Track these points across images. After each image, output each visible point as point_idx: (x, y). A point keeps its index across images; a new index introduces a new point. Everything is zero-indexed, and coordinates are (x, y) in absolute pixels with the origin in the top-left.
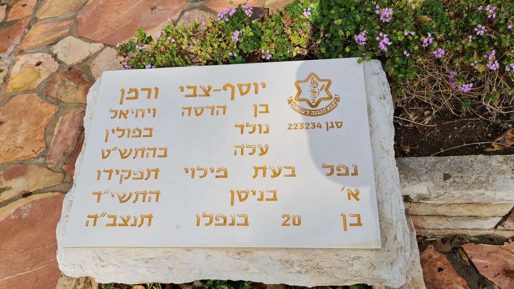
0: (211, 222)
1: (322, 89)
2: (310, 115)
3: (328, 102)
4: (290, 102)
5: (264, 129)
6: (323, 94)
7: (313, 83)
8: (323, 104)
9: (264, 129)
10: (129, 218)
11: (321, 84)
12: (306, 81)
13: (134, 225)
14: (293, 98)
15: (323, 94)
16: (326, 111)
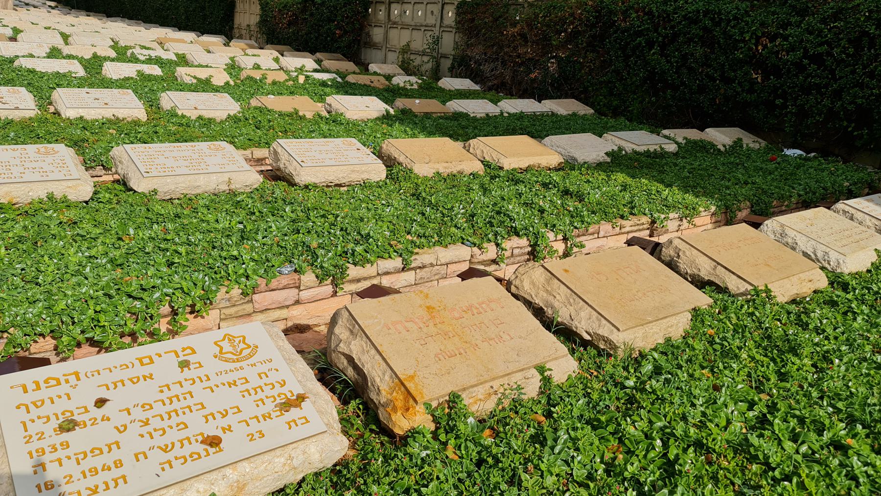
0: (186, 461)
1: (240, 342)
2: (238, 361)
3: (249, 350)
4: (216, 357)
5: (204, 378)
6: (242, 346)
7: (230, 340)
8: (246, 352)
9: (204, 378)
10: (97, 487)
11: (237, 340)
12: (224, 339)
13: (108, 488)
14: (218, 353)
15: (242, 346)
16: (250, 356)
